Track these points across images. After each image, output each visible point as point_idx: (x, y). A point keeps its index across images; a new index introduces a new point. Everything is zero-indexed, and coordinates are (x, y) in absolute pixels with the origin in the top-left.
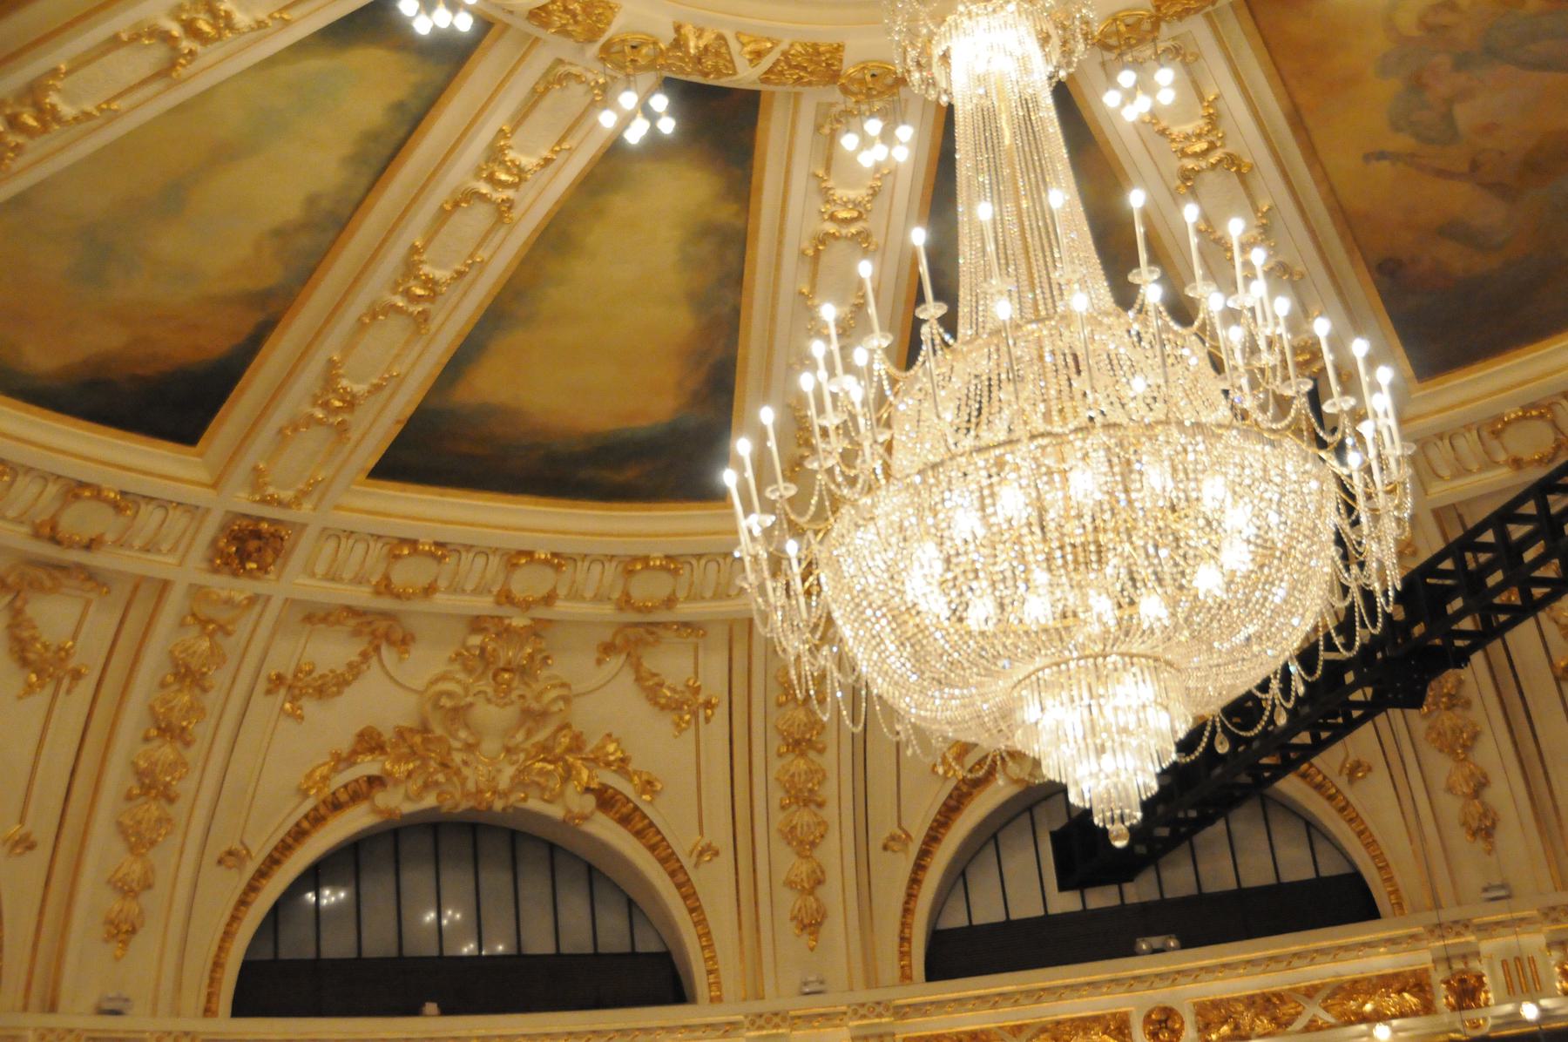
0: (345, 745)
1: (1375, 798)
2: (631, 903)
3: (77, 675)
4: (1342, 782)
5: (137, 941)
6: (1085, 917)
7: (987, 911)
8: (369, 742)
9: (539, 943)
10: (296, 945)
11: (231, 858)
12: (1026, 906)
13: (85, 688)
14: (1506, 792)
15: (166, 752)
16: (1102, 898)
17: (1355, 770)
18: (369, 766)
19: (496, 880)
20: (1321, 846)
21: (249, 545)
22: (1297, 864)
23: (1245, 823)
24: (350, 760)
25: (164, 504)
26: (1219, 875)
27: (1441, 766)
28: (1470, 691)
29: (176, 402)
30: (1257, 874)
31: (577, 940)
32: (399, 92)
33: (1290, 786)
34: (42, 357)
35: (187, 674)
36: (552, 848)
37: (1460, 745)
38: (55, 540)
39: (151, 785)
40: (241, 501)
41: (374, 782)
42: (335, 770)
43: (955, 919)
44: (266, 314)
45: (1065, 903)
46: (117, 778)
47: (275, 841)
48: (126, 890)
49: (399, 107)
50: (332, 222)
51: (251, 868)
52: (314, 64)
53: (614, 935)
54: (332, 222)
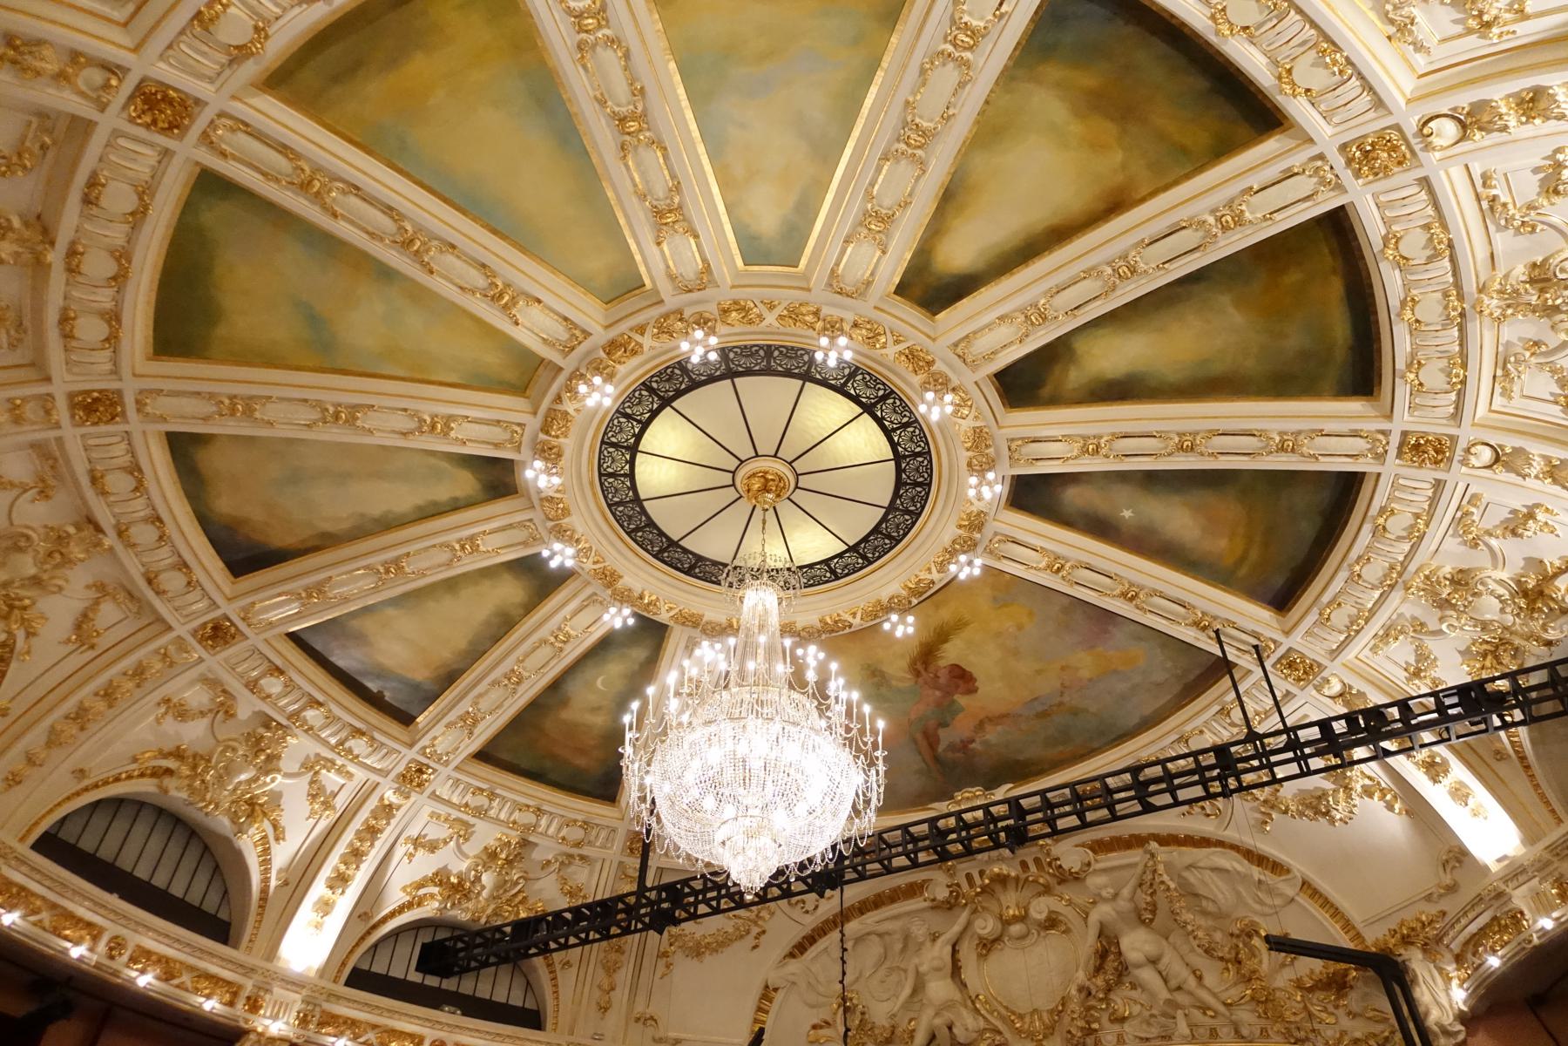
0: (168, 746)
1: (567, 979)
2: (226, 892)
3: (92, 647)
4: (558, 967)
5: (17, 788)
6: (420, 987)
7: (379, 968)
8: (178, 754)
9: (177, 890)
10: (68, 835)
11: (81, 773)
12: (397, 972)
13: (91, 654)
14: (620, 996)
15: (101, 705)
16: (432, 981)
17: (567, 964)
18: (170, 763)
19: (174, 850)
20: (529, 994)
21: (218, 634)
22: (516, 1000)
23: (505, 972)
24: (165, 756)
25: (205, 594)
26: (483, 992)
27: (601, 973)
28: (627, 948)
29: (246, 556)
30: (500, 996)
31: (194, 898)
32: (459, 493)
33: (539, 961)
34: (225, 505)
35: (139, 672)
36: (206, 848)
37: (611, 969)
38: (150, 582)
39: (80, 717)
40: (232, 610)
41: (169, 772)
42: (155, 758)
43: (365, 967)
44: (324, 542)
45: (415, 977)
46: (70, 705)
47: (104, 776)
48: (31, 760)
49: (456, 499)
50: (388, 524)
51: (86, 782)
52: (444, 465)
53: (210, 906)
54: (388, 524)
